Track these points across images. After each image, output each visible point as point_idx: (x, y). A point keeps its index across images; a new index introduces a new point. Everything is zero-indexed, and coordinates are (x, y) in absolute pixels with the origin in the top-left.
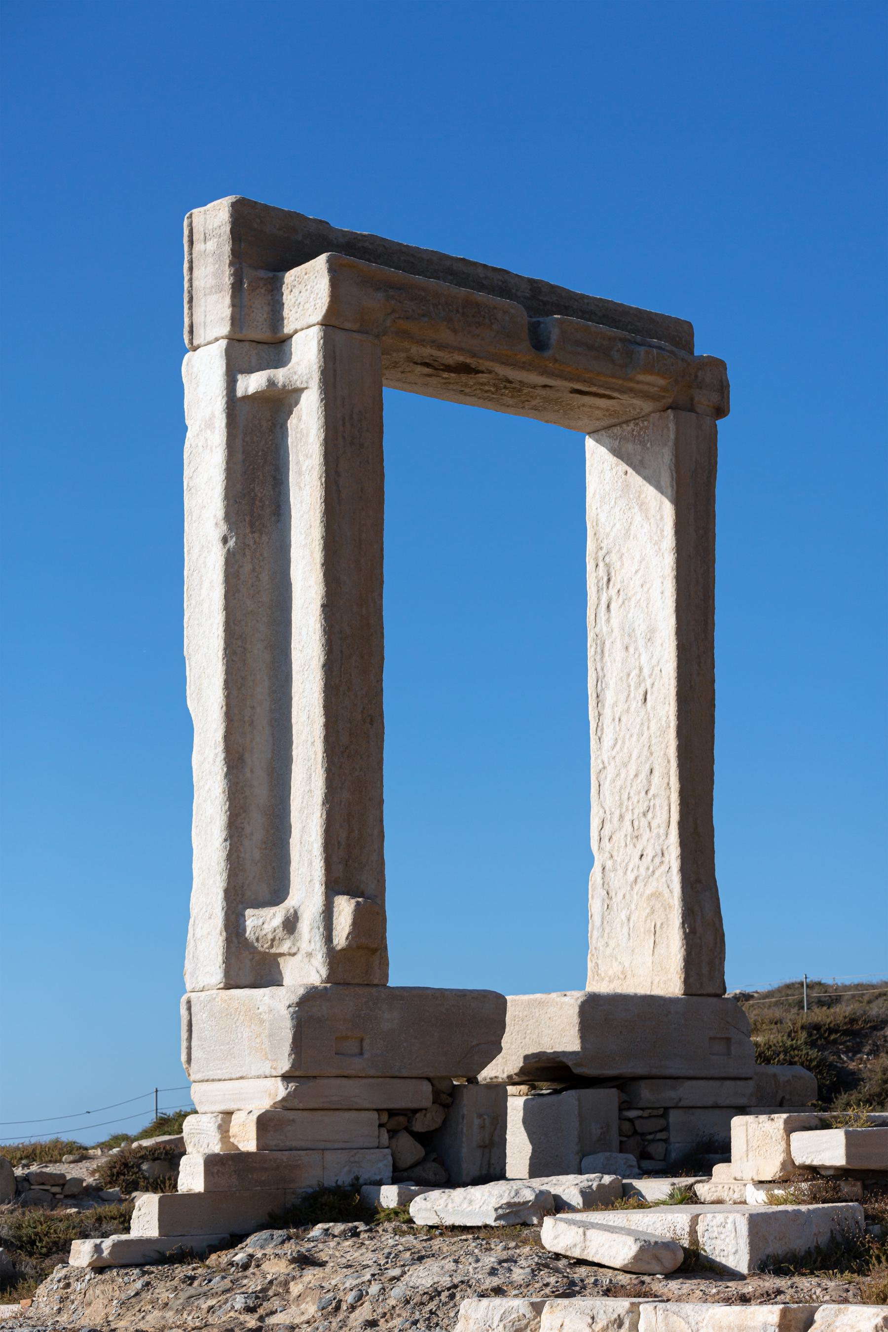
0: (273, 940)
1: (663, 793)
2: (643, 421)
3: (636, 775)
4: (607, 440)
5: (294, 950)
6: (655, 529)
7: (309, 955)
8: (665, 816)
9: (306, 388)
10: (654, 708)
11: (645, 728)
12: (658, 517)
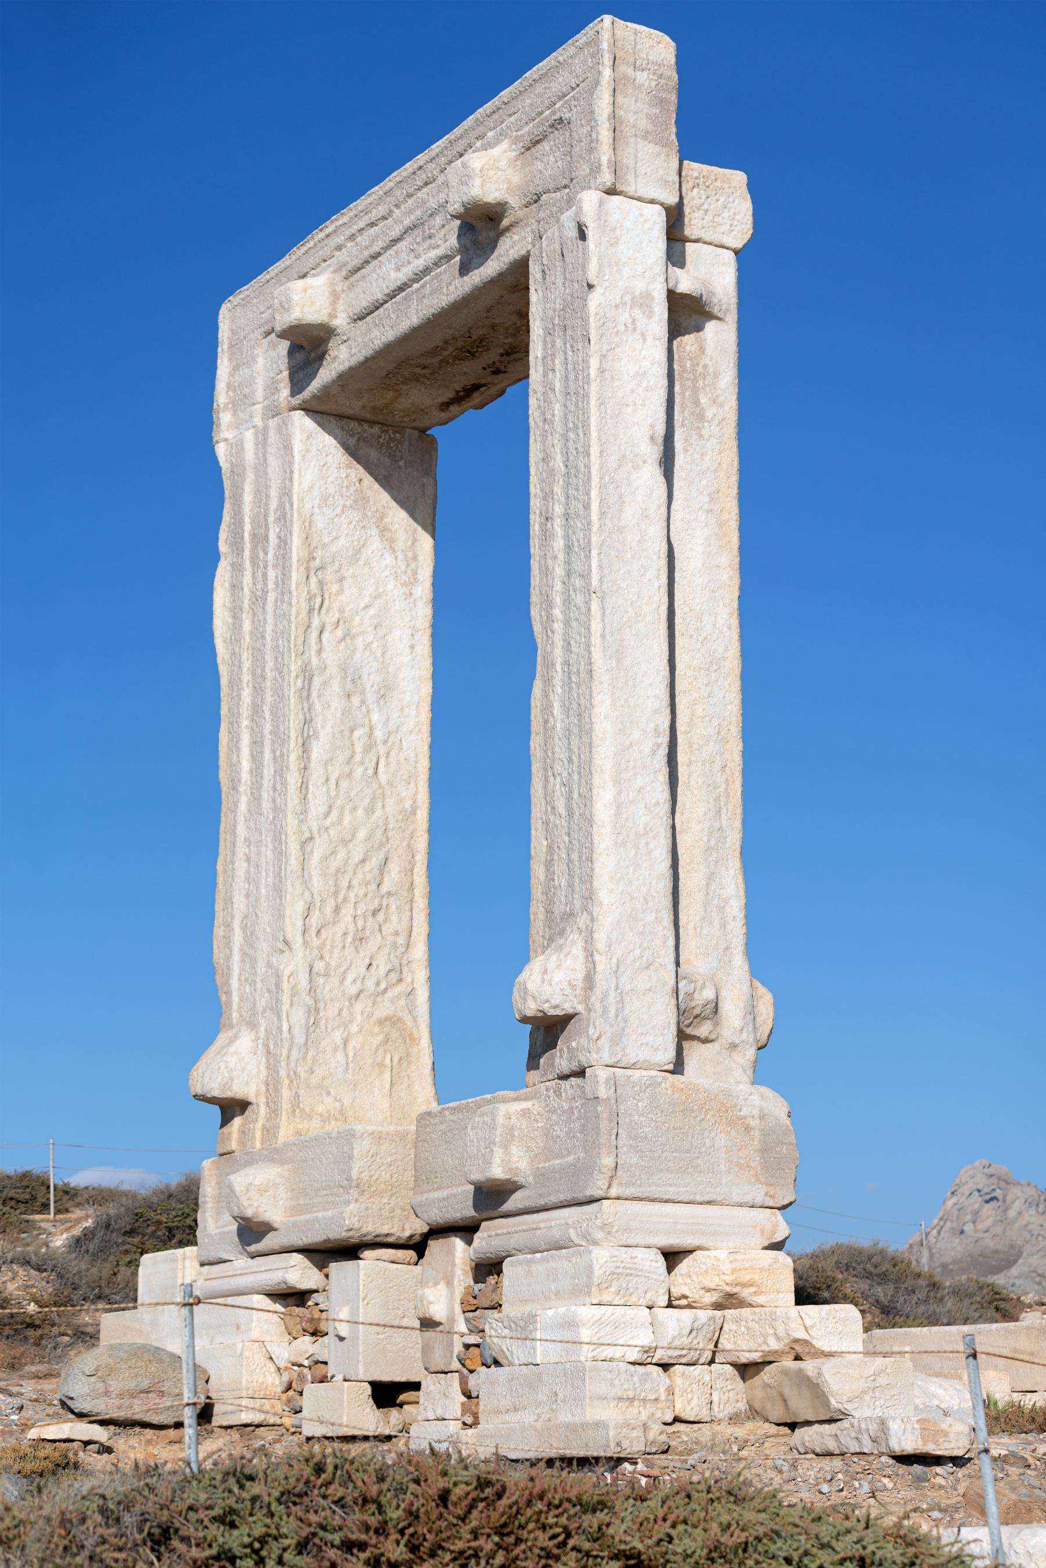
0: (696, 1017)
1: (405, 894)
2: (395, 432)
3: (363, 861)
4: (338, 431)
5: (712, 1037)
6: (403, 568)
7: (733, 1046)
8: (405, 925)
9: (720, 319)
10: (391, 784)
11: (380, 805)
12: (410, 555)
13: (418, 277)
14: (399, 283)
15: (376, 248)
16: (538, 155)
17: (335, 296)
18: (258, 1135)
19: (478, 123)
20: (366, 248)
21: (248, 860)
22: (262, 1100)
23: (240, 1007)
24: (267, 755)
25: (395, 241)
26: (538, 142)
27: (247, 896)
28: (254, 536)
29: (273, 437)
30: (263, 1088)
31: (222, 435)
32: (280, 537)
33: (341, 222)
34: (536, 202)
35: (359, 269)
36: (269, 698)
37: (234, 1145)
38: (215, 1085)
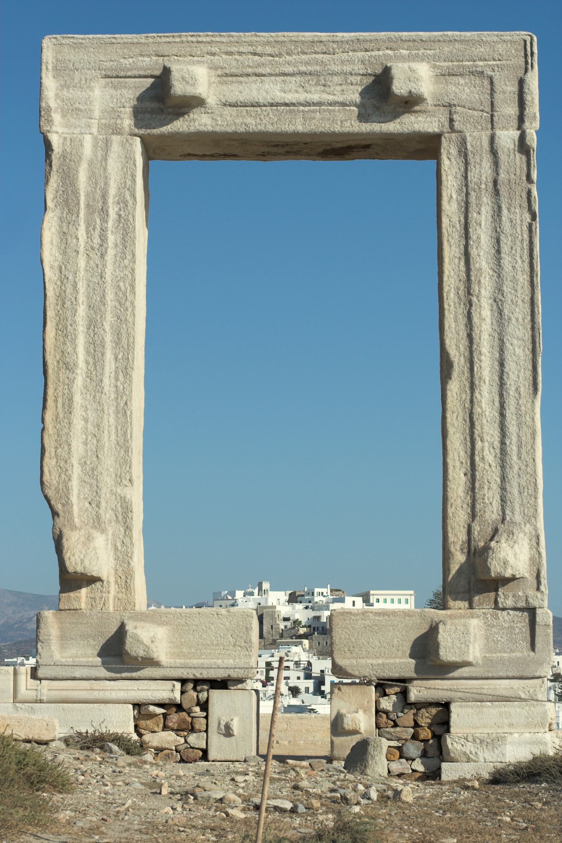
13: (308, 104)
14: (287, 101)
15: (260, 70)
16: (453, 82)
17: (210, 86)
18: (111, 601)
19: (390, 40)
20: (249, 67)
21: (86, 420)
22: (112, 580)
23: (80, 516)
24: (109, 355)
25: (285, 74)
26: (453, 75)
27: (85, 443)
28: (88, 206)
29: (116, 148)
30: (112, 572)
31: (54, 129)
32: (120, 216)
33: (218, 39)
34: (444, 106)
35: (237, 76)
36: (109, 319)
37: (83, 606)
38: (95, 568)
